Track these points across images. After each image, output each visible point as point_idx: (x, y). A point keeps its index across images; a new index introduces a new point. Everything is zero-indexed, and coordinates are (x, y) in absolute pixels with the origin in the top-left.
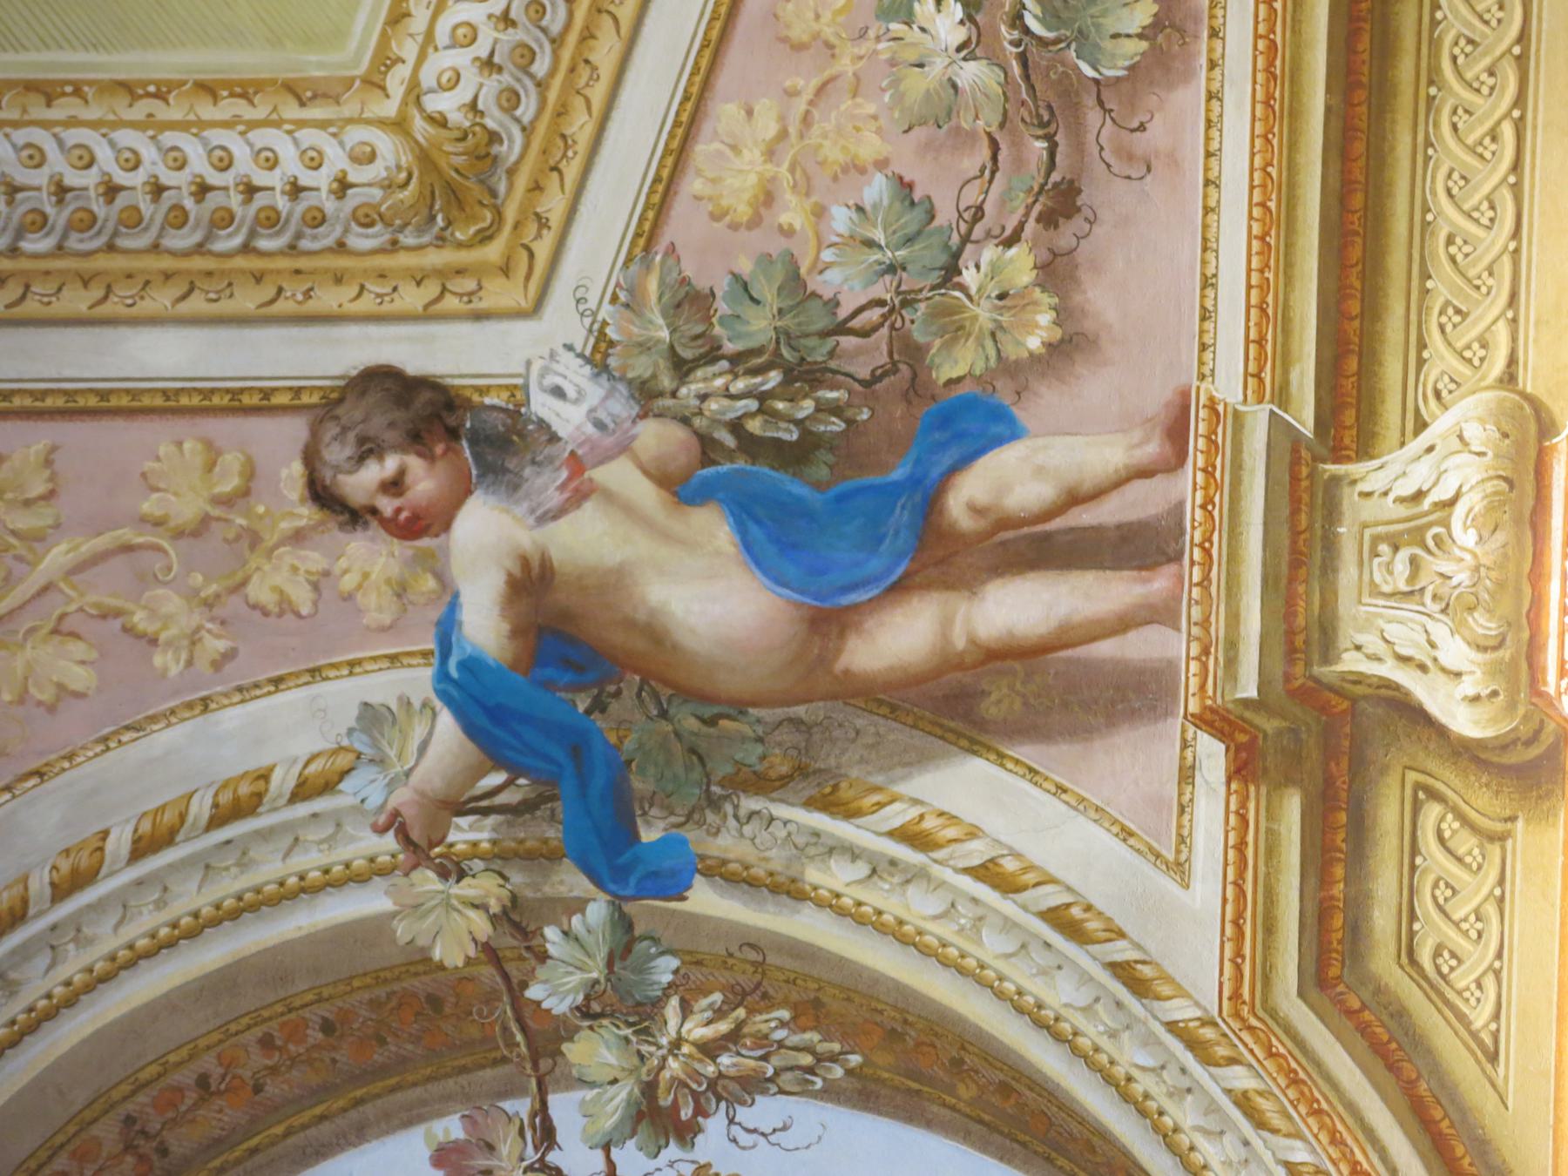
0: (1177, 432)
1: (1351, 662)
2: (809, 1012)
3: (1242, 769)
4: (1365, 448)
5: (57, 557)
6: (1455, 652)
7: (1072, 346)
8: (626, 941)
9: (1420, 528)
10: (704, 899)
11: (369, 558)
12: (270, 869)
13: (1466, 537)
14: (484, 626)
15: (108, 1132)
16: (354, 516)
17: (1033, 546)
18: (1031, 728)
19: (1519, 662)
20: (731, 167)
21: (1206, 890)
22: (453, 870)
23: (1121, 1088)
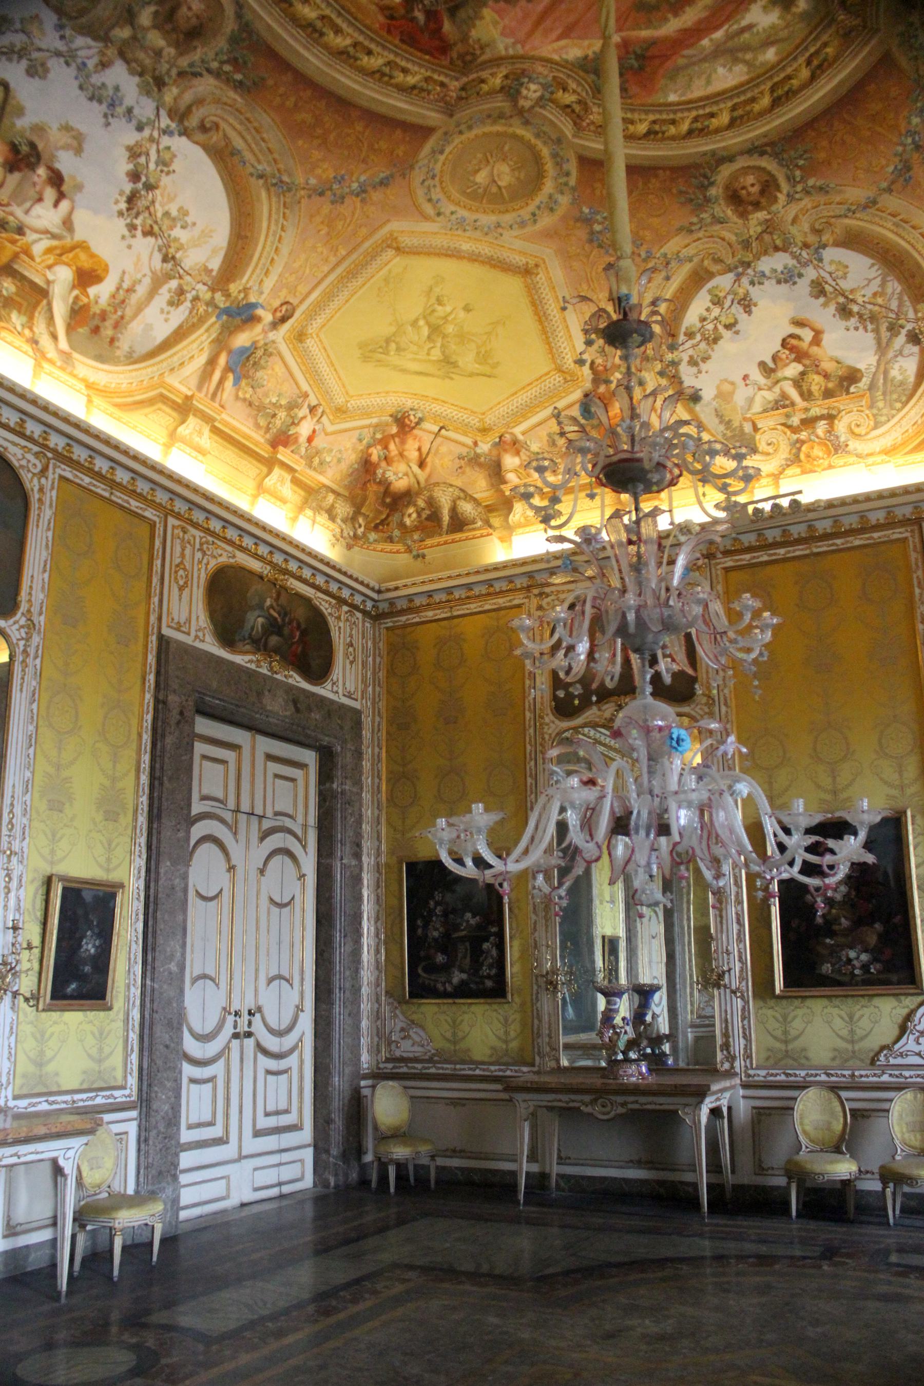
0: (222, 407)
1: (191, 417)
2: (193, 325)
3: (188, 398)
4: (211, 431)
5: (308, 271)
6: (187, 432)
7: (237, 397)
8: (216, 307)
9: (200, 433)
10: (214, 319)
11: (277, 303)
12: (258, 271)
13: (197, 439)
14: (260, 312)
15: (249, 234)
16: (282, 305)
17: (221, 382)
18: (204, 371)
19: (183, 441)
20: (279, 369)
21: (177, 385)
22: (240, 292)
23: (162, 361)
